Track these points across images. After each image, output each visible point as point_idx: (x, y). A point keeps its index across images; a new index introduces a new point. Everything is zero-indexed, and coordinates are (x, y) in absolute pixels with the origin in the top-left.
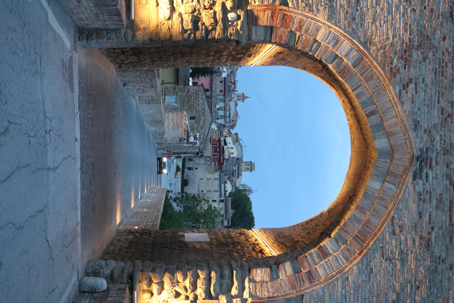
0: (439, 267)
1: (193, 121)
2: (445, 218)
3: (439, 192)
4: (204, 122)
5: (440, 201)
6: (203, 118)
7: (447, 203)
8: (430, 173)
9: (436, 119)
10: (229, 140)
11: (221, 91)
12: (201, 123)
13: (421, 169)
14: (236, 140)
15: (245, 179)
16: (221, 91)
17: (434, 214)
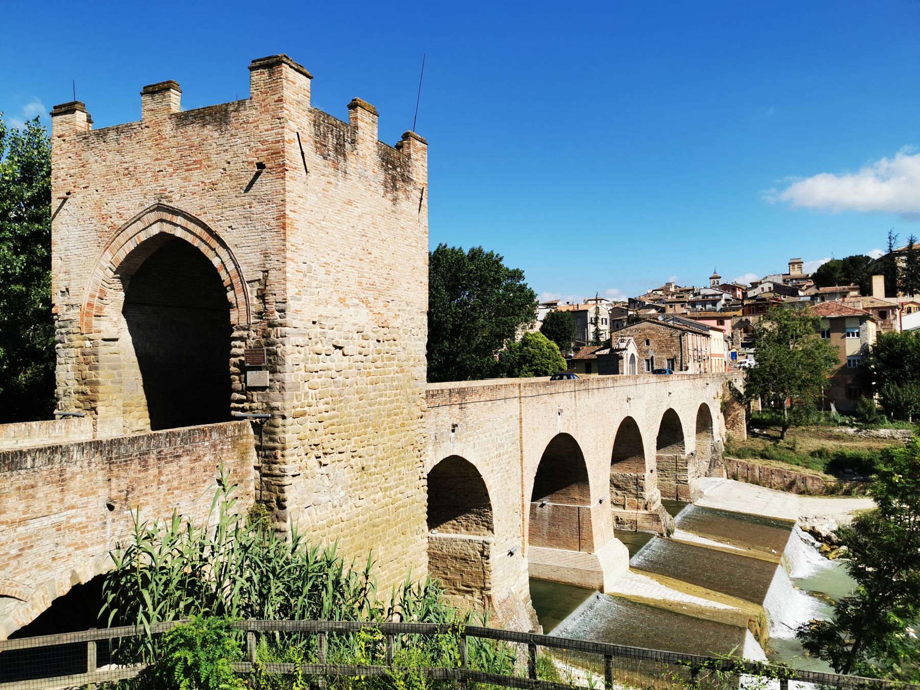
0: (228, 173)
1: (651, 342)
2: (195, 173)
3: (179, 180)
4: (652, 329)
5: (185, 179)
6: (648, 331)
7: (187, 173)
8: (169, 190)
9: (137, 190)
10: (750, 294)
11: (682, 306)
12: (652, 332)
13: (166, 197)
14: (755, 285)
15: (811, 268)
16: (682, 306)
17: (193, 183)
